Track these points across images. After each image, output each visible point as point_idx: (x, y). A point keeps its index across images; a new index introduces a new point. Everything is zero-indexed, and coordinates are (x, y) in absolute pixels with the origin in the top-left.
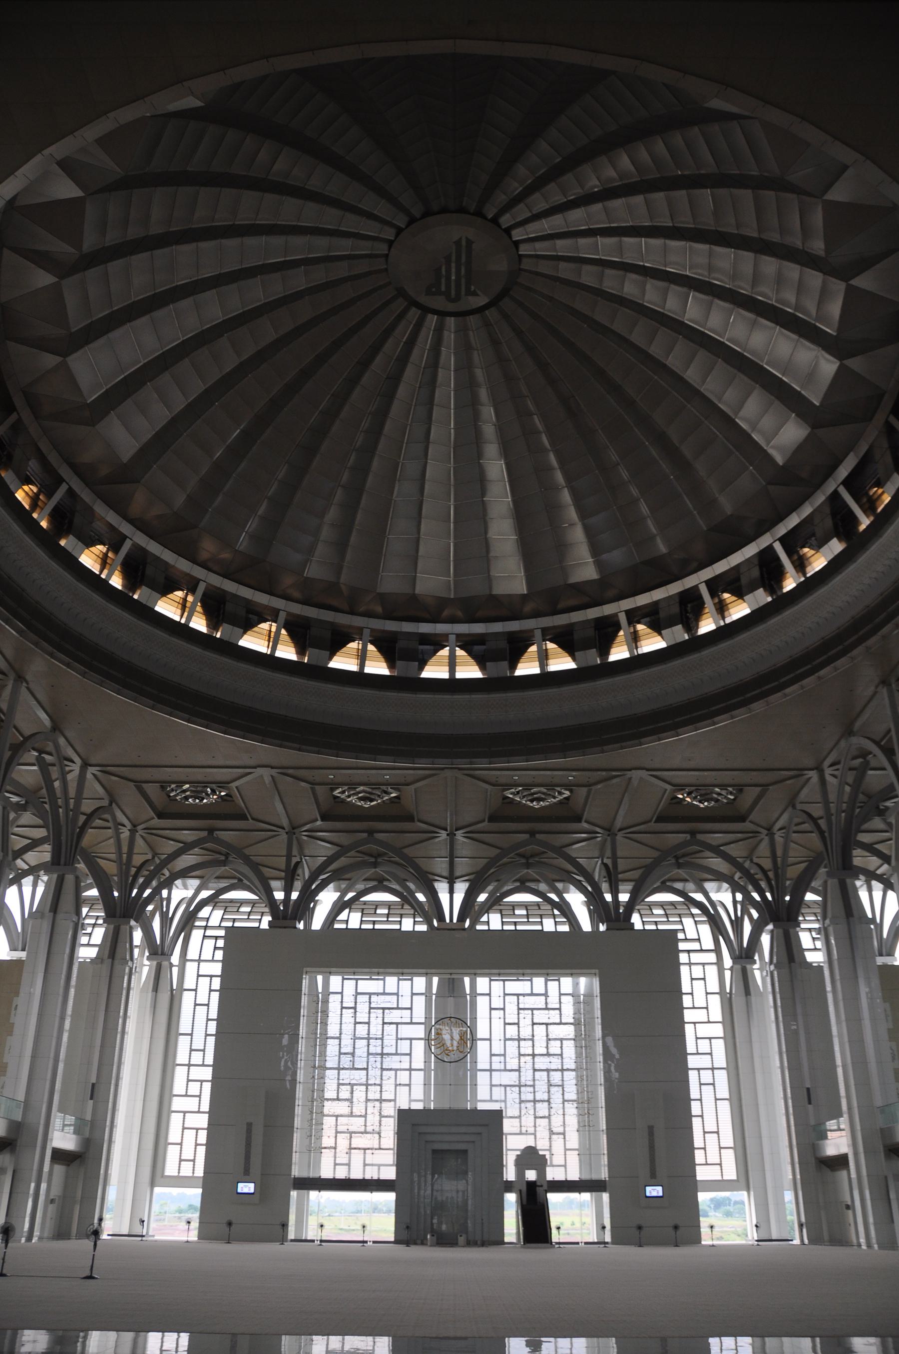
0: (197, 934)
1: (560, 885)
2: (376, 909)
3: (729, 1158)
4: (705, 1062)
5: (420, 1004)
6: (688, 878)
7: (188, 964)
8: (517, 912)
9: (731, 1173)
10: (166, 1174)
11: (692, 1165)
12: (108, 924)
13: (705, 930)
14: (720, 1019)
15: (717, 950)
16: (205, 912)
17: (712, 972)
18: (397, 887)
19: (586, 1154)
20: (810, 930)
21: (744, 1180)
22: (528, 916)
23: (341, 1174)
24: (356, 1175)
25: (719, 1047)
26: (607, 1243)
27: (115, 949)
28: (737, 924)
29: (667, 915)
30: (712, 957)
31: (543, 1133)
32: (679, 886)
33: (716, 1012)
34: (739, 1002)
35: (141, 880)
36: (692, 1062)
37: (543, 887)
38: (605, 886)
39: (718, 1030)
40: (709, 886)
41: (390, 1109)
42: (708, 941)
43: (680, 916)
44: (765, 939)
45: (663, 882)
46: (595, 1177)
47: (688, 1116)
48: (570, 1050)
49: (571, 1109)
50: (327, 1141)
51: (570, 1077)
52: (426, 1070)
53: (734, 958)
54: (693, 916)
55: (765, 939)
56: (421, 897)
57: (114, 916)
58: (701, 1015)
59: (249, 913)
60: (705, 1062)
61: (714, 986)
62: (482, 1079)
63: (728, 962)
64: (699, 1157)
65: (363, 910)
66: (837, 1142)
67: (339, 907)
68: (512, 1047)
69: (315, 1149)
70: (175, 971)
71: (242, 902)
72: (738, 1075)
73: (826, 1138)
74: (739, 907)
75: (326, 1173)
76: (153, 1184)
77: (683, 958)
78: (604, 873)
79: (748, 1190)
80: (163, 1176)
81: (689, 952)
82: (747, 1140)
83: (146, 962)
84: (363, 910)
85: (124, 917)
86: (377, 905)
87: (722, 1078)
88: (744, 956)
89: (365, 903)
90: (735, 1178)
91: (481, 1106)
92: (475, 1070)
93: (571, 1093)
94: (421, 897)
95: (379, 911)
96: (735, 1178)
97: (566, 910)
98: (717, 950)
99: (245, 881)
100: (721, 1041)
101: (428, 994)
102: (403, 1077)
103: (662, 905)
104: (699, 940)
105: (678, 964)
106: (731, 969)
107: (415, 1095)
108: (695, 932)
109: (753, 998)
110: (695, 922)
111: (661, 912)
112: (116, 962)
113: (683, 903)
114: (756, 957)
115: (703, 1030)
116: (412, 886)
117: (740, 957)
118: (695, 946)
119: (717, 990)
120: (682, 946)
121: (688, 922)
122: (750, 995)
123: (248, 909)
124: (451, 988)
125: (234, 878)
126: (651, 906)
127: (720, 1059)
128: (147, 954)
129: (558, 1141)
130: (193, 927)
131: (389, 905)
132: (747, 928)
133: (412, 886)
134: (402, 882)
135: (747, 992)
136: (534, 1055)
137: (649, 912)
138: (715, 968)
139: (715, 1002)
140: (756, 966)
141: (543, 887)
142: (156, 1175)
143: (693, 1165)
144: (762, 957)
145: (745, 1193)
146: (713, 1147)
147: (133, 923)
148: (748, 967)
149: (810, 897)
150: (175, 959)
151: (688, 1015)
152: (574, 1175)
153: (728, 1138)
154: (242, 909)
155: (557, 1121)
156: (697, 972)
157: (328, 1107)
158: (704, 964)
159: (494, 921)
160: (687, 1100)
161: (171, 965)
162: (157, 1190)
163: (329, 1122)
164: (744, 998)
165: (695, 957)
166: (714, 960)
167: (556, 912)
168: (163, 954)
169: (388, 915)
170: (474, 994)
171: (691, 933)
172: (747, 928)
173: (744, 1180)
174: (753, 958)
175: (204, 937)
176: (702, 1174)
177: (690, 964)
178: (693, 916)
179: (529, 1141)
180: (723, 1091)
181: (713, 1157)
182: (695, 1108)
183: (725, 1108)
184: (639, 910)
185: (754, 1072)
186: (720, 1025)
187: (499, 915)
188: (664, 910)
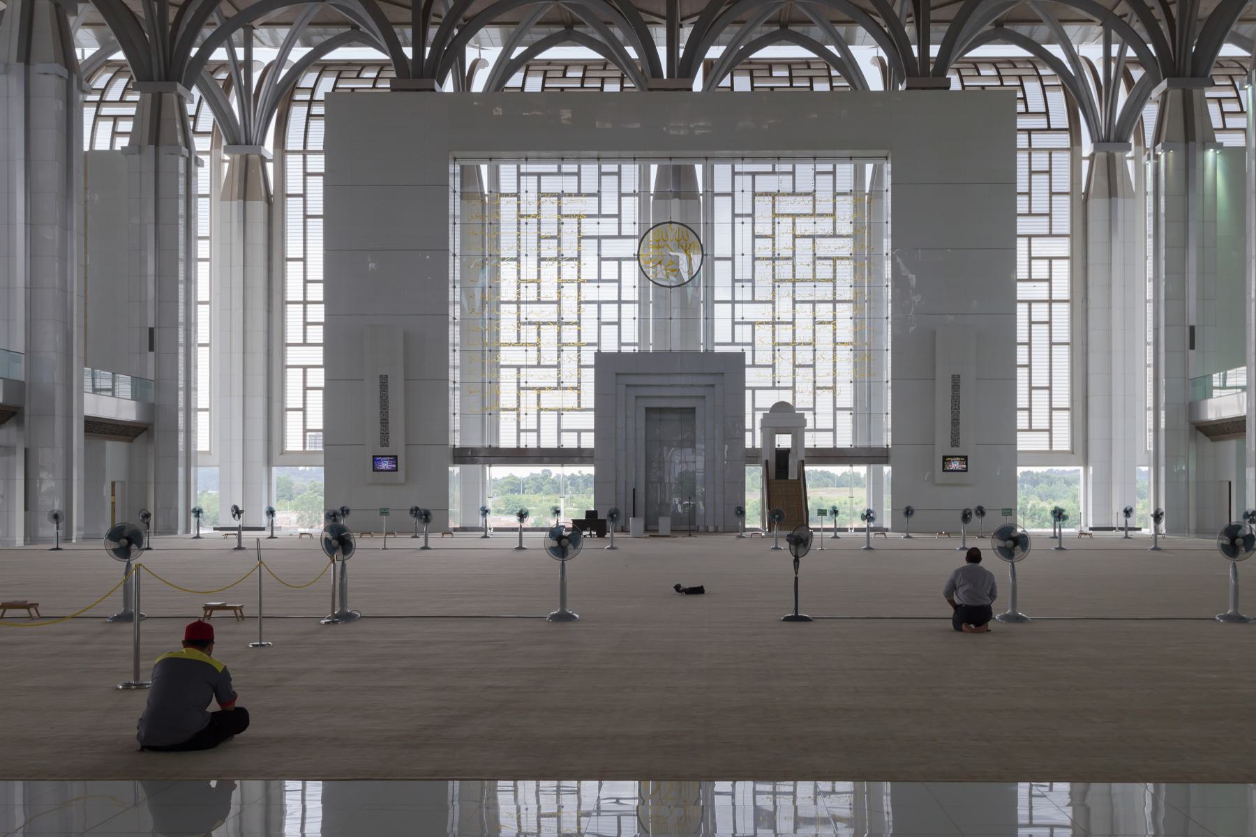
0: (298, 114)
1: (841, 30)
2: (565, 72)
3: (1062, 422)
4: (1041, 291)
5: (631, 207)
6: (1041, 16)
7: (290, 158)
8: (775, 74)
9: (1062, 442)
10: (288, 449)
11: (1011, 431)
12: (143, 92)
13: (1058, 101)
14: (1067, 231)
15: (1074, 130)
16: (308, 80)
17: (1062, 162)
18: (597, 37)
19: (863, 412)
20: (1219, 100)
21: (1081, 451)
22: (791, 78)
23: (529, 441)
24: (549, 442)
25: (1062, 271)
26: (887, 530)
27: (160, 132)
28: (1108, 91)
29: (1000, 77)
30: (1064, 140)
31: (804, 387)
32: (1023, 30)
33: (1062, 222)
34: (1097, 206)
35: (207, 32)
36: (1023, 291)
37: (816, 33)
38: (910, 30)
39: (1061, 247)
40: (1071, 30)
41: (589, 357)
42: (1060, 117)
43: (1020, 77)
44: (1150, 113)
45: (999, 24)
46: (874, 444)
47: (1011, 366)
48: (846, 271)
49: (845, 354)
50: (507, 397)
51: (845, 311)
52: (642, 302)
53: (1096, 140)
54: (1040, 77)
55: (1150, 113)
56: (632, 52)
57: (150, 79)
58: (1041, 225)
59: (376, 80)
60: (1041, 291)
61: (1062, 181)
62: (722, 313)
63: (1087, 148)
64: (1022, 420)
65: (545, 72)
66: (1224, 403)
67: (505, 68)
68: (764, 269)
69: (489, 411)
70: (270, 167)
71: (363, 65)
72: (1086, 311)
73: (1211, 396)
74: (1113, 65)
75: (507, 440)
76: (269, 462)
77: (1022, 141)
78: (911, 10)
79: (1086, 465)
80: (283, 452)
81: (1029, 132)
82: (1091, 400)
83: (227, 157)
84: (545, 72)
85: (167, 79)
86: (566, 65)
87: (1062, 313)
88: (1114, 138)
89: (549, 62)
90: (1067, 448)
91: (718, 349)
92: (711, 302)
93: (846, 331)
94: (632, 52)
95: (569, 74)
96: (1067, 448)
97: (849, 67)
98: (1074, 130)
99: (363, 29)
100: (1066, 263)
101: (642, 194)
102: (610, 312)
103: (994, 62)
104: (1047, 113)
105: (1015, 150)
106: (1092, 158)
107: (626, 334)
108: (1043, 100)
109: (1120, 201)
110: (1043, 87)
111: (993, 72)
112: (162, 150)
113: (1027, 60)
114: (1132, 140)
115: (1040, 247)
116: (618, 33)
117: (1107, 140)
118: (1041, 123)
119: (1067, 189)
120: (1022, 123)
121: (1033, 88)
122: (1116, 196)
123: (374, 75)
124: (678, 184)
125: (345, 24)
126: (976, 64)
127: (1062, 288)
128: (224, 143)
129: (825, 399)
130: (290, 101)
131: (585, 65)
132: (1123, 97)
133: (618, 33)
134: (603, 26)
135: (1112, 192)
136: (794, 281)
137: (973, 72)
138: (1067, 155)
139: (1063, 207)
140: (1130, 154)
141: (816, 33)
142: (273, 451)
143: (1013, 431)
144: (1140, 141)
145: (1081, 469)
146: (1042, 409)
147: (180, 88)
148: (1118, 154)
149: (1229, 50)
150: (269, 146)
151: (1023, 226)
152: (845, 440)
153: (1062, 396)
154: (366, 74)
155: (824, 368)
156: (1040, 161)
157: (508, 355)
158: (1050, 151)
159: (742, 83)
160: (1012, 344)
161: (263, 160)
162: (275, 470)
163: (507, 378)
164: (1106, 201)
165: (1038, 141)
166: (1068, 145)
167: (834, 73)
168: (248, 142)
169: (583, 79)
170: (711, 194)
171: (1036, 103)
172: (1123, 97)
173: (1081, 451)
174: (1126, 141)
175: (309, 116)
176: (1025, 442)
177: (1030, 150)
178: (1040, 77)
179: (786, 397)
180: (1062, 331)
181: (1040, 420)
182: (1022, 355)
183: (1062, 356)
184: (958, 70)
185: (1110, 307)
186: (1067, 241)
187: (748, 78)
188: (998, 70)
